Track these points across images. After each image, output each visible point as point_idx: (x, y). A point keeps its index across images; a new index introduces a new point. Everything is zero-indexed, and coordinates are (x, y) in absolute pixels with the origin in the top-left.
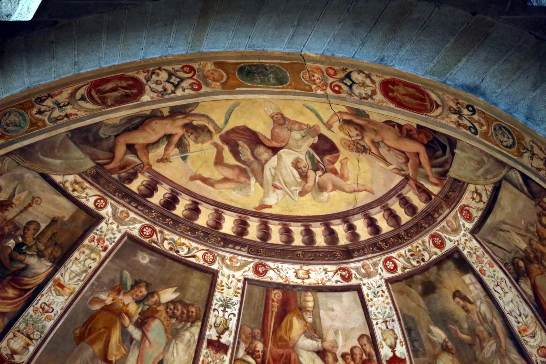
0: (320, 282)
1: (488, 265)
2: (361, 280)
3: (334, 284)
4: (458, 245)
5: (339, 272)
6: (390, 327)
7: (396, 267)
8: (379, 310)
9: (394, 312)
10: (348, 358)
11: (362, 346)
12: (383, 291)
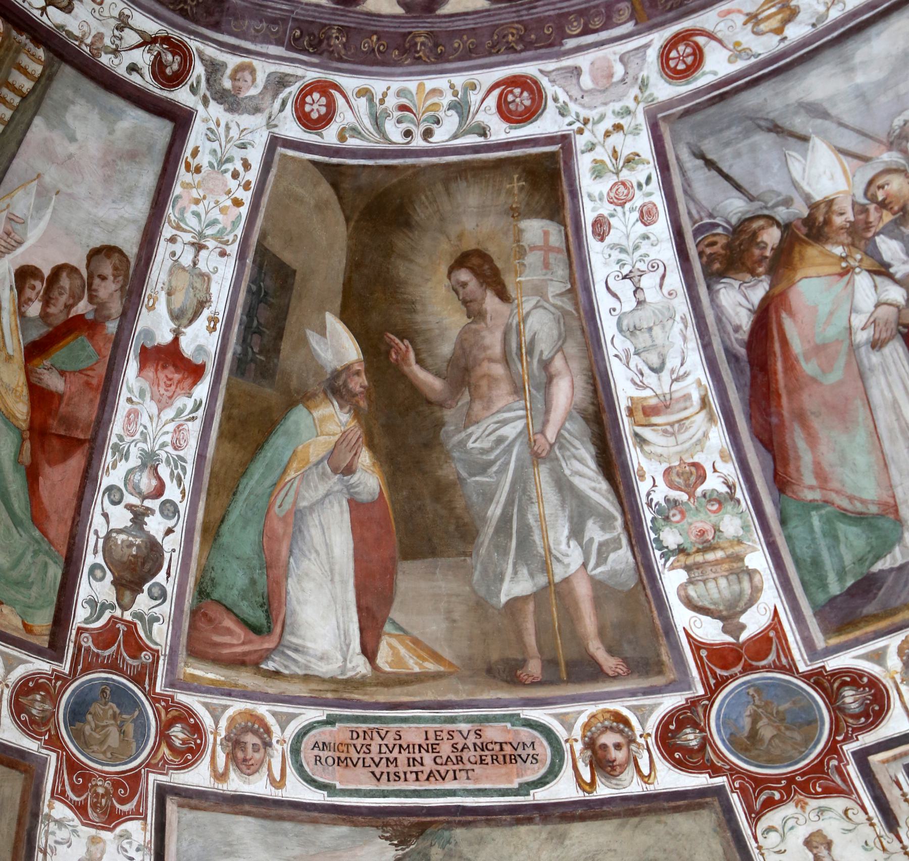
0: (88, 41)
1: (636, 215)
2: (205, 102)
3: (121, 71)
4: (581, 131)
5: (157, 47)
6: (202, 266)
7: (326, 119)
8: (200, 208)
9: (239, 232)
10: (34, 288)
11: (91, 276)
12: (247, 165)
